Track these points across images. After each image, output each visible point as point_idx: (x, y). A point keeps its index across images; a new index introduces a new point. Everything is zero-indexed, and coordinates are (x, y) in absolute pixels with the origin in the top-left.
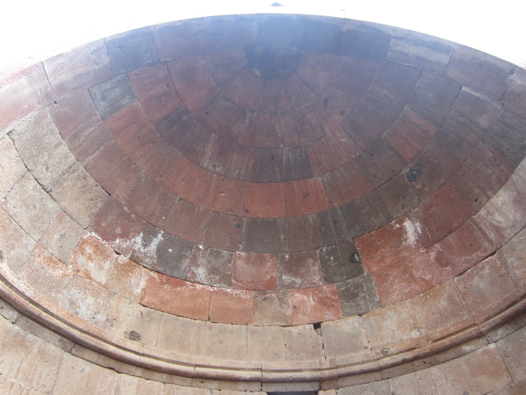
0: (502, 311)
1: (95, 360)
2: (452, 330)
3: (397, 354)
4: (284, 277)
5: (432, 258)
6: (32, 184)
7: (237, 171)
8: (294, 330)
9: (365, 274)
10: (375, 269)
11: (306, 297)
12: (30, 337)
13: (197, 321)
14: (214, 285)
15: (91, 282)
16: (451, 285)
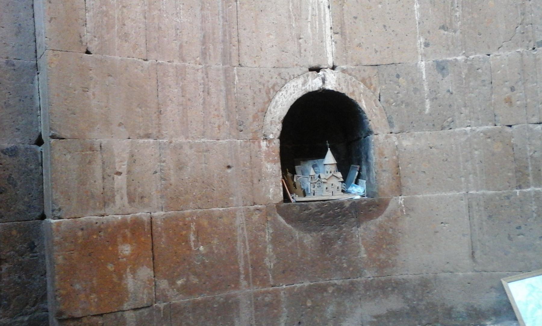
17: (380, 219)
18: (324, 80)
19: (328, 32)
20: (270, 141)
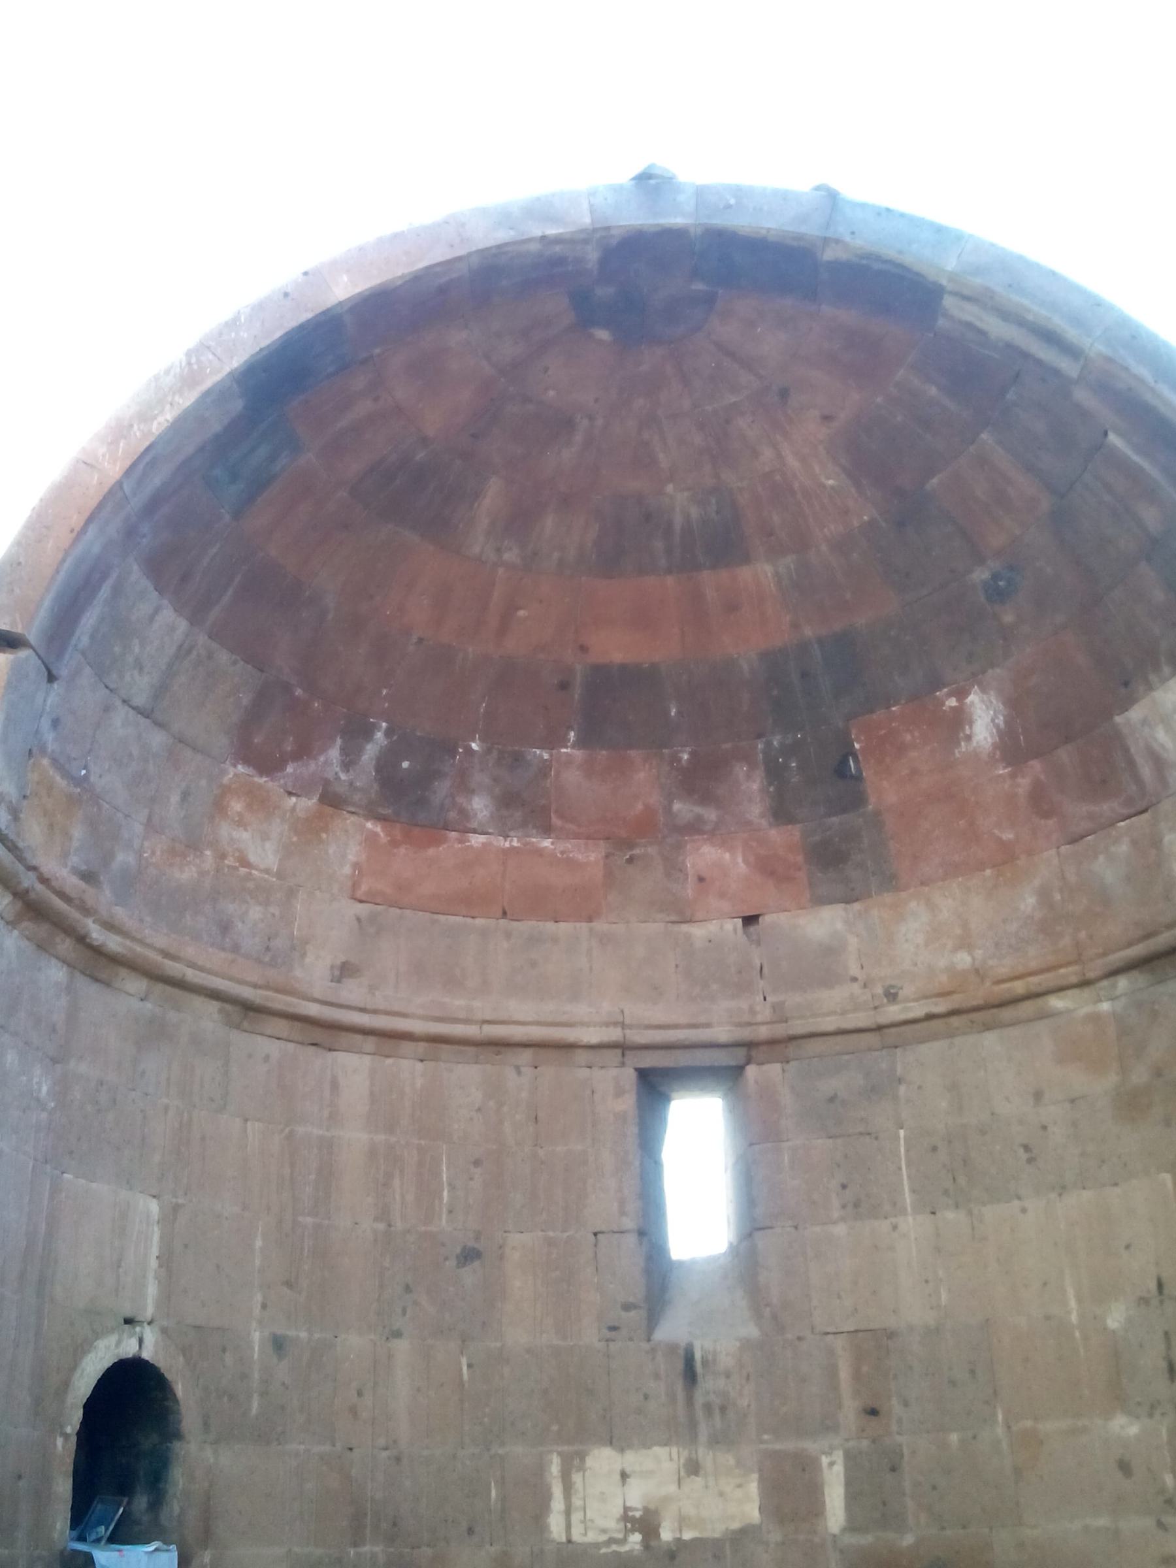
0: (1130, 944)
1: (285, 1035)
2: (1033, 965)
3: (916, 1000)
4: (677, 806)
5: (1020, 791)
7: (556, 555)
8: (698, 932)
9: (870, 807)
10: (891, 798)
11: (727, 856)
12: (172, 1016)
13: (479, 922)
14: (512, 833)
15: (250, 874)
16: (1049, 863)
18: (141, 1341)
19: (153, 1263)
20: (66, 1436)
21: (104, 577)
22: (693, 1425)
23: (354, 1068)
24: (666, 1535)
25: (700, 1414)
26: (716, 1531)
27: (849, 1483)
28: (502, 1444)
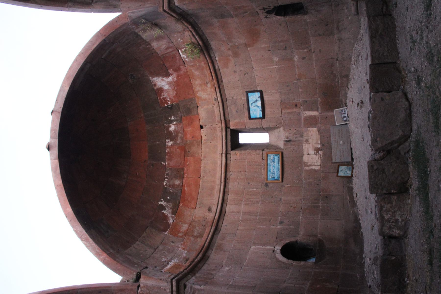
2: (209, 72)
6: (155, 255)
8: (204, 138)
17: (324, 241)
19: (264, 247)
21: (127, 257)
22: (299, 140)
23: (229, 208)
24: (319, 146)
25: (297, 139)
26: (318, 136)
27: (309, 111)
28: (302, 178)
